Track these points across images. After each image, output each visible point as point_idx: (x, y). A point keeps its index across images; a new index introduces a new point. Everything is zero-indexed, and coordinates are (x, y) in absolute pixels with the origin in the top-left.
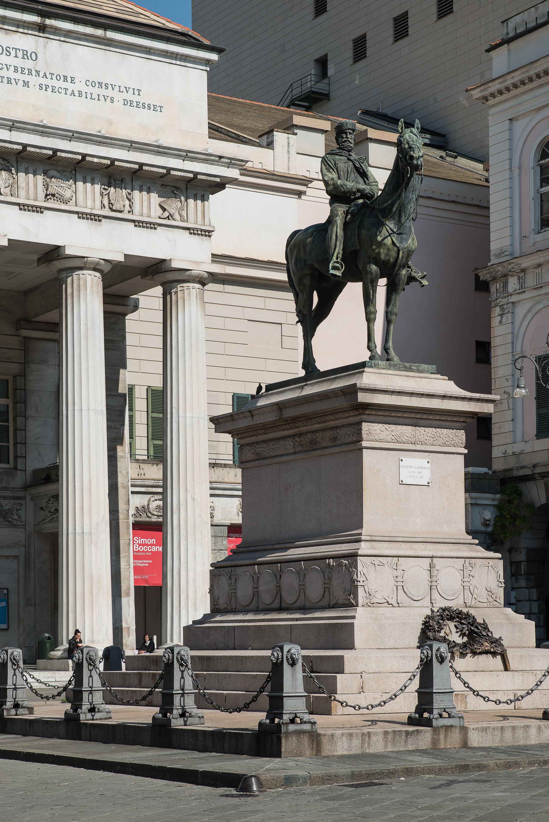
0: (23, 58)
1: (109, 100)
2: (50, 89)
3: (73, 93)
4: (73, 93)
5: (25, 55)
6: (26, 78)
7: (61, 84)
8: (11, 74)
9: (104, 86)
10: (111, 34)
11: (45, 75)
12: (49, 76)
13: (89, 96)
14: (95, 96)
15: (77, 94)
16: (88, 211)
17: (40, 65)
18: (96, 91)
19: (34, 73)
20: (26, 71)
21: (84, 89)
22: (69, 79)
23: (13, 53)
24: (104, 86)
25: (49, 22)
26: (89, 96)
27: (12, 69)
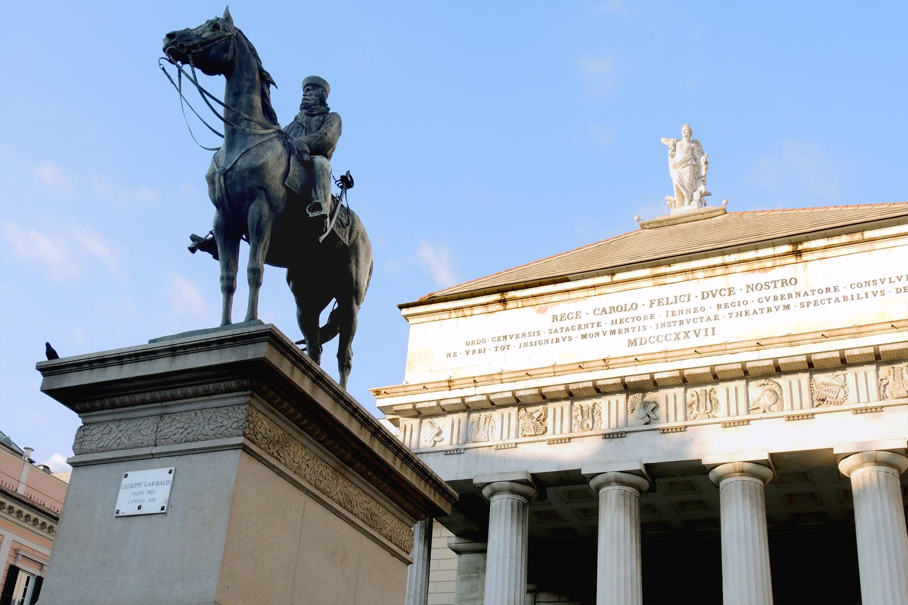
0: (783, 286)
1: (879, 294)
2: (813, 303)
3: (837, 300)
4: (837, 300)
5: (784, 283)
6: (786, 302)
7: (825, 296)
8: (772, 304)
9: (871, 283)
10: (868, 234)
11: (806, 293)
12: (810, 293)
13: (855, 297)
14: (862, 295)
15: (841, 299)
16: (862, 405)
17: (801, 287)
18: (862, 291)
19: (794, 295)
20: (786, 296)
21: (849, 292)
22: (832, 289)
23: (772, 285)
24: (871, 283)
25: (800, 247)
26: (855, 297)
27: (772, 298)
